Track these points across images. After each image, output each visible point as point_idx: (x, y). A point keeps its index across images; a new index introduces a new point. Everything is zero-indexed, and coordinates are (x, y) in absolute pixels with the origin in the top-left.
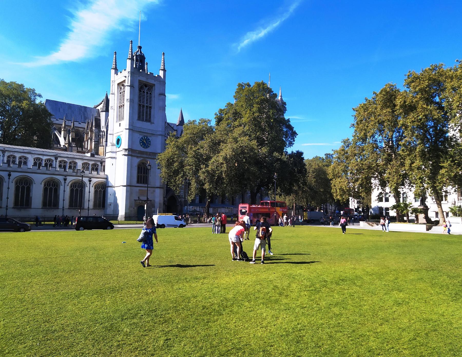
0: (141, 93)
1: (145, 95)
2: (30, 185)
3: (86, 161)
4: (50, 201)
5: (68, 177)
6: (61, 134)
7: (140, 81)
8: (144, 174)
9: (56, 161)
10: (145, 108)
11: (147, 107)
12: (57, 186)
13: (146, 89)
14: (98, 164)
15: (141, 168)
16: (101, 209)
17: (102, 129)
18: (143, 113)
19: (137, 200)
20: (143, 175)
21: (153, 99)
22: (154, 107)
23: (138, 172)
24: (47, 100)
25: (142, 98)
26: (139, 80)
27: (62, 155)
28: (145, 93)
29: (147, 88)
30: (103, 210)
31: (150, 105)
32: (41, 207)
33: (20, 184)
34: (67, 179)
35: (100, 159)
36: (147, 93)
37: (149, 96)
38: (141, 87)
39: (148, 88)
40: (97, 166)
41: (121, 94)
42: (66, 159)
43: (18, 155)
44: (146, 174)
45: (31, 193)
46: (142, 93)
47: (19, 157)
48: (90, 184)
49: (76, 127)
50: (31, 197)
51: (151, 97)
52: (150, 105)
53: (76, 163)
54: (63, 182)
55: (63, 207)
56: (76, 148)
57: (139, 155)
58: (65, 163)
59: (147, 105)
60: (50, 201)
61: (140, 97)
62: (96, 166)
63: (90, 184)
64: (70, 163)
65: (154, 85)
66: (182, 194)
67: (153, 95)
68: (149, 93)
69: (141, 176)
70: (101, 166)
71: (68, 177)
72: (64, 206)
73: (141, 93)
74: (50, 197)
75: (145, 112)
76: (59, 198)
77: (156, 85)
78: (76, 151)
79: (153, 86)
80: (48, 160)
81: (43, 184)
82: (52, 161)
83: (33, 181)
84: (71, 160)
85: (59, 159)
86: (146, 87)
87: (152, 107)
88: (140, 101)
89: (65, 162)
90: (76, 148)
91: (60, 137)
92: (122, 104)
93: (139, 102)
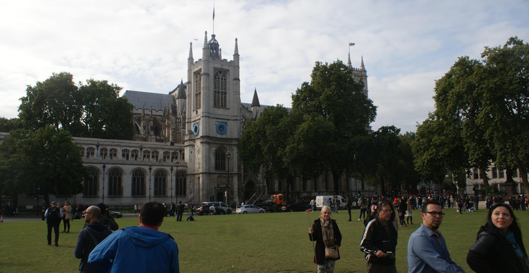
0: (216, 80)
1: (220, 81)
2: (121, 175)
3: (166, 150)
5: (152, 167)
6: (140, 123)
7: (215, 69)
9: (141, 152)
10: (220, 94)
11: (222, 92)
12: (143, 175)
13: (220, 76)
14: (177, 153)
15: (219, 154)
16: (182, 197)
17: (178, 116)
18: (219, 98)
19: (216, 187)
21: (228, 85)
22: (229, 93)
23: (216, 159)
24: (127, 91)
25: (217, 84)
26: (214, 68)
27: (146, 146)
28: (220, 80)
29: (222, 74)
30: (184, 198)
31: (225, 91)
32: (130, 196)
33: (117, 176)
34: (152, 169)
35: (179, 148)
36: (222, 79)
37: (224, 82)
38: (216, 73)
39: (223, 75)
40: (176, 154)
41: (198, 82)
42: (149, 150)
43: (109, 148)
44: (225, 160)
45: (122, 183)
46: (217, 79)
47: (110, 149)
48: (172, 172)
49: (154, 115)
50: (123, 187)
51: (226, 83)
52: (225, 91)
53: (157, 153)
54: (148, 171)
55: (150, 196)
56: (155, 136)
57: (216, 142)
58: (148, 153)
59: (222, 91)
61: (215, 84)
62: (175, 154)
63: (172, 172)
64: (153, 153)
65: (228, 70)
66: (260, 179)
67: (228, 80)
68: (224, 79)
69: (219, 163)
70: (180, 154)
71: (152, 167)
72: (151, 195)
73: (216, 80)
75: (220, 98)
76: (145, 187)
77: (230, 71)
78: (154, 140)
79: (227, 72)
80: (134, 151)
81: (132, 174)
82: (138, 151)
83: (123, 171)
84: (153, 150)
85: (144, 150)
86: (220, 74)
87: (227, 92)
88: (215, 88)
89: (149, 152)
90: (155, 136)
91: (140, 126)
92: (198, 92)
93: (215, 89)
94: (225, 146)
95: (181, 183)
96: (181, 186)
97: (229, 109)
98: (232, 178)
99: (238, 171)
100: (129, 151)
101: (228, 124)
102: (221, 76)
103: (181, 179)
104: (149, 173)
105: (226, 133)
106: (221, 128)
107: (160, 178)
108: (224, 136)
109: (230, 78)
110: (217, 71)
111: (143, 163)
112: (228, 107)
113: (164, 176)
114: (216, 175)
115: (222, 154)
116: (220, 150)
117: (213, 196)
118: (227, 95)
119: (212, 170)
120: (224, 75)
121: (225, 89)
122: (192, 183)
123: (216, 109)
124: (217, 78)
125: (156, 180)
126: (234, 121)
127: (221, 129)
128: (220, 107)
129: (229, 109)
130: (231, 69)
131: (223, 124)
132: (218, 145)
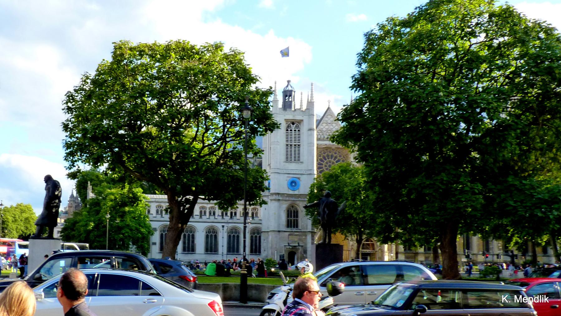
4: (211, 247)
8: (294, 217)
11: (295, 145)
12: (216, 233)
13: (293, 127)
15: (291, 211)
20: (293, 218)
21: (301, 136)
28: (293, 132)
29: (295, 125)
52: (299, 143)
54: (221, 228)
59: (295, 143)
60: (211, 247)
61: (287, 136)
65: (302, 120)
68: (297, 130)
69: (291, 220)
74: (211, 243)
88: (287, 141)
94: (298, 202)
95: (256, 240)
96: (256, 244)
97: (302, 162)
98: (306, 236)
99: (312, 229)
100: (206, 207)
101: (301, 179)
102: (293, 128)
103: (256, 237)
104: (222, 231)
105: (298, 189)
106: (293, 184)
107: (234, 236)
108: (296, 192)
109: (304, 128)
110: (289, 123)
111: (215, 221)
112: (301, 160)
113: (238, 234)
114: (287, 234)
115: (294, 211)
116: (293, 207)
117: (284, 255)
118: (301, 148)
119: (283, 227)
120: (297, 127)
121: (299, 141)
122: (265, 241)
123: (287, 164)
124: (289, 130)
125: (229, 237)
126: (309, 176)
127: (293, 184)
128: (293, 161)
129: (302, 162)
130: (305, 119)
131: (295, 179)
132: (289, 203)
